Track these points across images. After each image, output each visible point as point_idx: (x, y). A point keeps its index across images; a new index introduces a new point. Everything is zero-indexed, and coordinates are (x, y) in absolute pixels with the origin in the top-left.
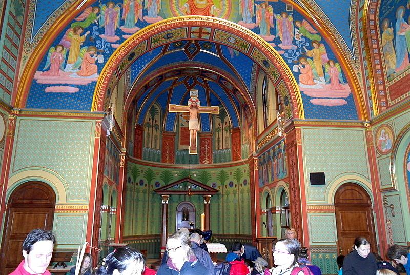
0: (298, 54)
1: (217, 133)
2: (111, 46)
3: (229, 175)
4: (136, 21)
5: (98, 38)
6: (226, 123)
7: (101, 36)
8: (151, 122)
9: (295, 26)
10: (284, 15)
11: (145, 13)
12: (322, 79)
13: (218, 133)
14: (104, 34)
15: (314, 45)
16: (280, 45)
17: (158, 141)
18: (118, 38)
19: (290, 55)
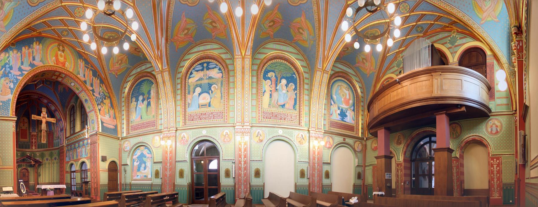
0: (100, 100)
2: (17, 78)
4: (29, 63)
5: (9, 72)
7: (11, 71)
9: (100, 86)
10: (96, 78)
11: (34, 59)
12: (108, 115)
14: (12, 70)
15: (107, 98)
16: (94, 94)
18: (20, 73)
19: (97, 100)
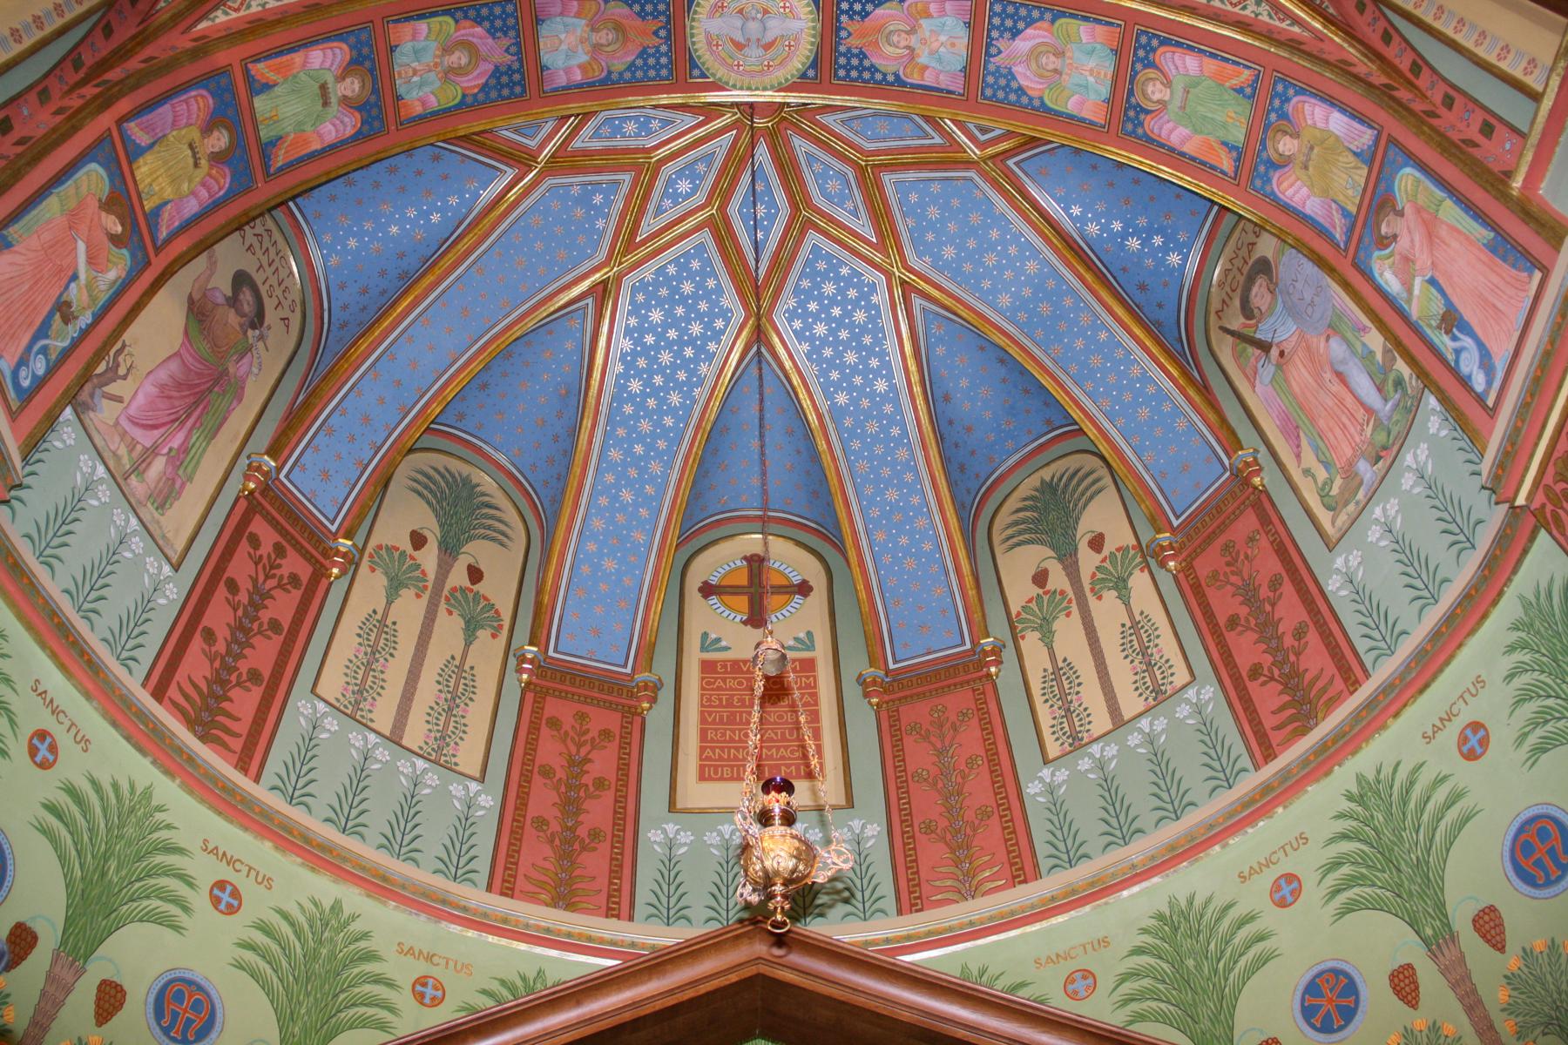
1: (1031, 643)
3: (1271, 918)
6: (1097, 543)
8: (429, 558)
13: (1047, 637)
17: (477, 714)
